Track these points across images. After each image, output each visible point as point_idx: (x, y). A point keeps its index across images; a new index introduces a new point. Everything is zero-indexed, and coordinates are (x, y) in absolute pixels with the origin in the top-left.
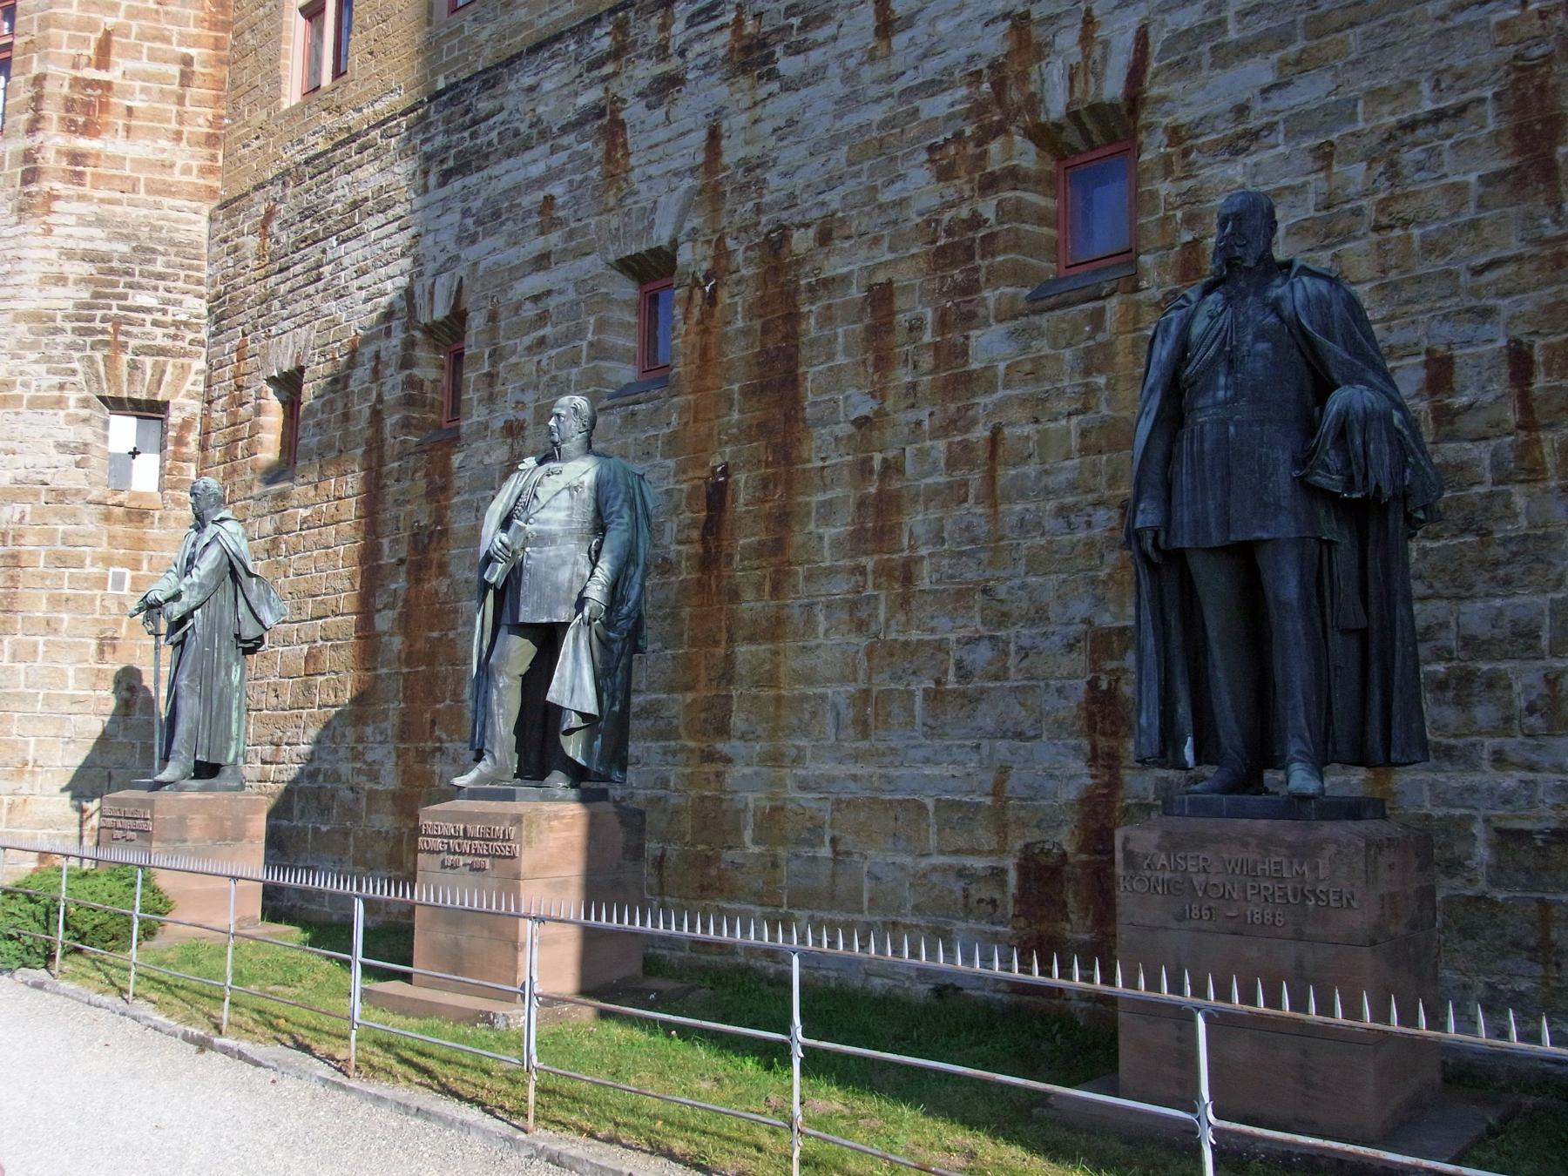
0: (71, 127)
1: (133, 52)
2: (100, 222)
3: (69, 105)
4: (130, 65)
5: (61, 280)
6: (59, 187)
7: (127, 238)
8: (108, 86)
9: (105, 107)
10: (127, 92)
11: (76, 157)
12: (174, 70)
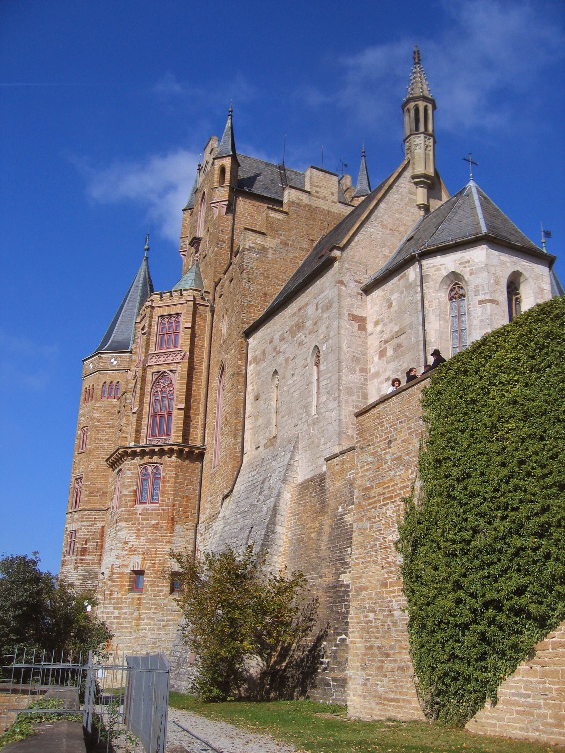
0: (82, 555)
1: (90, 542)
2: (84, 570)
3: (81, 551)
5: (79, 579)
8: (86, 548)
9: (86, 551)
10: (89, 548)
11: (82, 560)
12: (95, 544)
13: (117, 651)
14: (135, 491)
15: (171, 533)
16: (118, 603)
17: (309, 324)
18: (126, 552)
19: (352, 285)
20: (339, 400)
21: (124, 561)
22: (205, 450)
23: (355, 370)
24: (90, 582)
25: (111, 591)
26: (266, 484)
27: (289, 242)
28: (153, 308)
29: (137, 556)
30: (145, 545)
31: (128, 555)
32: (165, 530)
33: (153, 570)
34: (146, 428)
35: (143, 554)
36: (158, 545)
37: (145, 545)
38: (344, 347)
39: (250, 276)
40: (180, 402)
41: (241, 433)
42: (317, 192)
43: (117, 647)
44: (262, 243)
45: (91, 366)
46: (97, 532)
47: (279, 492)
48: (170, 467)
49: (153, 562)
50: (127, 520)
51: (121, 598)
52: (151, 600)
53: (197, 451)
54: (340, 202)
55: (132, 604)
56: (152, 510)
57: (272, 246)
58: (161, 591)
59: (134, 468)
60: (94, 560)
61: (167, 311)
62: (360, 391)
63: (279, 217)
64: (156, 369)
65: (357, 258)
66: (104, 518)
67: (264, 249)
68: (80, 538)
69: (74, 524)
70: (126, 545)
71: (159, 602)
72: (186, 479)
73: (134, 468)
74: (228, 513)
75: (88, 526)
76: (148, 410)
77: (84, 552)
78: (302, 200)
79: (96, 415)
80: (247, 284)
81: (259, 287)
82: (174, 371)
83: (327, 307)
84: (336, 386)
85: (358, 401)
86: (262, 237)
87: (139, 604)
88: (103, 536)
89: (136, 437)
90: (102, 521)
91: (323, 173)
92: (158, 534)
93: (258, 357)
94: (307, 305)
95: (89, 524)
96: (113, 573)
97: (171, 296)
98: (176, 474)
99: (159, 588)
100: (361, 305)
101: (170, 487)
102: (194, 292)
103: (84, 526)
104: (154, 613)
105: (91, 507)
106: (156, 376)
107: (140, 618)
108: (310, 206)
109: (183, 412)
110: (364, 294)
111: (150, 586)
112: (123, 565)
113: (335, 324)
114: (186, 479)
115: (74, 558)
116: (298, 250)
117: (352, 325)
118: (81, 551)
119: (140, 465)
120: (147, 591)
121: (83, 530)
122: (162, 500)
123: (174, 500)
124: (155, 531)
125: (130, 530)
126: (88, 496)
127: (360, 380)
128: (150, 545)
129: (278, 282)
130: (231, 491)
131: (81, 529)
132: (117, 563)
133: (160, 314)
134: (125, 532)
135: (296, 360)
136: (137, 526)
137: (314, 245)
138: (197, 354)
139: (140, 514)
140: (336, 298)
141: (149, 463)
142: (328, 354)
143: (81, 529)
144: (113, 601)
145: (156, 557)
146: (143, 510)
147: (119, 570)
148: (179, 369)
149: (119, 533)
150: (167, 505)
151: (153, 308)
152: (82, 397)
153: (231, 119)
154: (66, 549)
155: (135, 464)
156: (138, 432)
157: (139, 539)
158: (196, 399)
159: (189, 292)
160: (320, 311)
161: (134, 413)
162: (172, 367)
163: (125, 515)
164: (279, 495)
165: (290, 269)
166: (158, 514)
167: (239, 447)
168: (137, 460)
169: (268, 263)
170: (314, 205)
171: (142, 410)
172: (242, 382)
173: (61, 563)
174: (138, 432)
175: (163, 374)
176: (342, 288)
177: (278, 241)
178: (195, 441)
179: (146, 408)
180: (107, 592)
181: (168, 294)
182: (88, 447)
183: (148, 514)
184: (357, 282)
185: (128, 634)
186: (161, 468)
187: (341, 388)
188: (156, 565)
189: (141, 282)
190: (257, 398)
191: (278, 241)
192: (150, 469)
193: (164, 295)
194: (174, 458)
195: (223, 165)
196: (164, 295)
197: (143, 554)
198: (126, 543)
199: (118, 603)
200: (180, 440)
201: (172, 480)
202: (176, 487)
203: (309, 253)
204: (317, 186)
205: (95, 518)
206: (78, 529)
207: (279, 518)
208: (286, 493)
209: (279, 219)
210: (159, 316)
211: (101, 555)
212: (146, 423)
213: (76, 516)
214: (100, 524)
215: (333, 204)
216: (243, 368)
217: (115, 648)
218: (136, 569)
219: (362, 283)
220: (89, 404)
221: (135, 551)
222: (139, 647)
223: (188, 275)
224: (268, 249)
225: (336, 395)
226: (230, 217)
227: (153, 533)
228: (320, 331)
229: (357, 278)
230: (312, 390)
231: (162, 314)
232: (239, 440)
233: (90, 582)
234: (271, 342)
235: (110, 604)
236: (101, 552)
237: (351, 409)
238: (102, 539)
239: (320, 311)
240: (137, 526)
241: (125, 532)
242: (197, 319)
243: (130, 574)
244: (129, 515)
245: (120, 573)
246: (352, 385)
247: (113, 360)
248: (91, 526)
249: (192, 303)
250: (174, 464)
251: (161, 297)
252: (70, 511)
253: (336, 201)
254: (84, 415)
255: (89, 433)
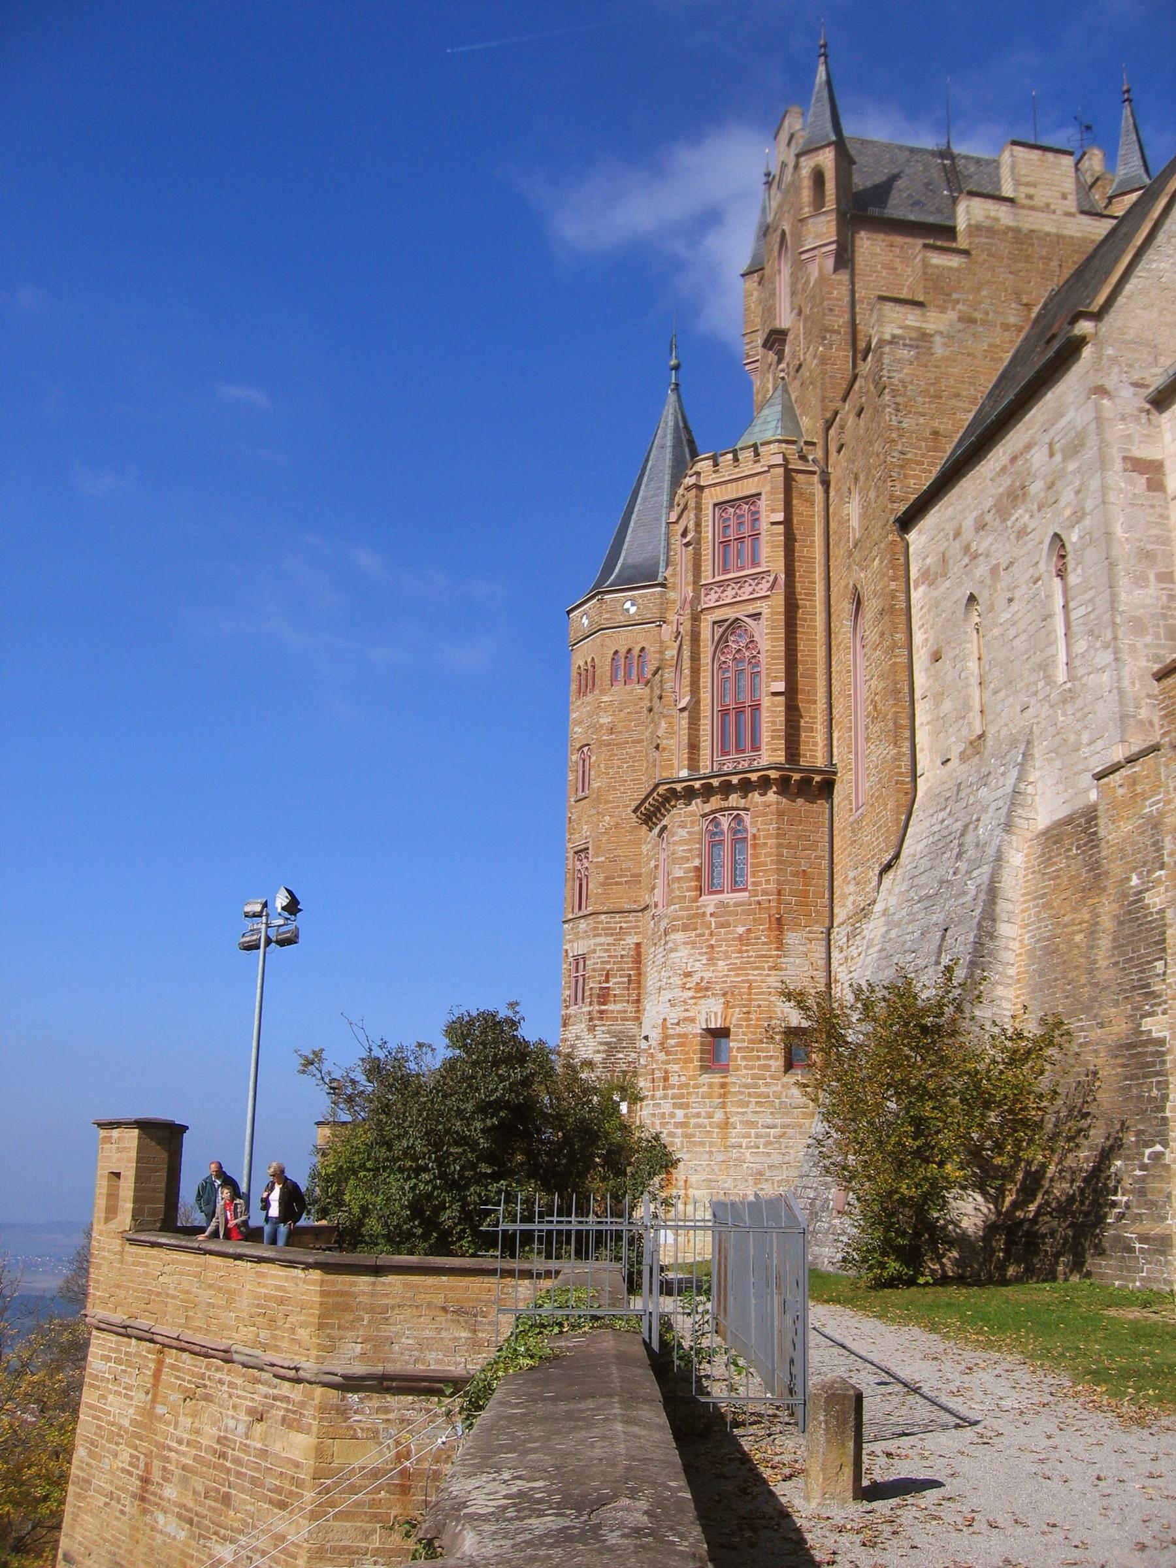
1: (615, 976)
2: (608, 1032)
3: (599, 996)
4: (615, 980)
5: (599, 1052)
6: (597, 1022)
7: (614, 1037)
8: (608, 988)
9: (608, 995)
10: (614, 989)
11: (601, 1012)
12: (626, 979)
13: (686, 1189)
14: (698, 869)
15: (778, 949)
16: (682, 1096)
17: (1036, 488)
18: (690, 994)
19: (1127, 392)
20: (1115, 648)
21: (687, 1010)
22: (835, 773)
23: (1148, 579)
24: (621, 1056)
25: (666, 1072)
26: (970, 838)
27: (978, 316)
28: (700, 488)
29: (712, 1000)
30: (727, 976)
31: (694, 998)
32: (764, 943)
33: (748, 1026)
34: (709, 738)
35: (724, 995)
36: (753, 975)
37: (727, 976)
38: (1119, 531)
39: (899, 399)
40: (775, 679)
41: (907, 734)
42: (1030, 197)
43: (686, 1181)
44: (917, 324)
45: (585, 621)
46: (628, 956)
47: (999, 851)
48: (764, 814)
49: (745, 1010)
50: (685, 928)
51: (687, 1085)
52: (747, 1086)
53: (818, 778)
54: (1083, 212)
55: (710, 1096)
56: (737, 905)
57: (942, 328)
58: (766, 1067)
59: (693, 822)
60: (626, 1011)
61: (731, 492)
62: (1161, 623)
63: (951, 264)
64: (718, 615)
65: (1132, 331)
66: (636, 927)
67: (924, 337)
68: (594, 970)
69: (581, 942)
70: (689, 979)
71: (763, 1089)
72: (799, 838)
73: (693, 822)
74: (893, 901)
75: (608, 944)
76: (709, 700)
77: (604, 996)
78: (997, 220)
79: (605, 720)
80: (894, 418)
81: (922, 420)
82: (756, 616)
83: (1074, 449)
84: (1107, 617)
85: (1159, 646)
86: (918, 311)
87: (724, 1095)
88: (639, 962)
89: (690, 759)
90: (636, 933)
91: (1039, 152)
92: (751, 953)
93: (932, 571)
94: (1028, 447)
95: (610, 940)
96: (666, 1037)
97: (736, 459)
98: (779, 828)
99: (763, 1062)
100: (1149, 436)
101: (769, 855)
102: (784, 445)
103: (600, 944)
104: (756, 1112)
105: (611, 907)
106: (721, 630)
107: (727, 1123)
108: (1017, 230)
109: (782, 699)
110: (1153, 411)
111: (744, 1058)
112: (685, 1019)
113: (1094, 484)
114: (799, 838)
115: (586, 1009)
116: (998, 329)
117: (1131, 482)
118: (599, 996)
119: (704, 816)
120: (738, 1069)
121: (598, 954)
122: (755, 884)
123: (779, 882)
124: (744, 948)
125: (693, 948)
126: (603, 884)
127: (1158, 598)
128: (737, 975)
129: (960, 404)
130: (897, 856)
131: (594, 951)
132: (674, 1015)
133: (716, 501)
134: (684, 952)
135: (1014, 568)
136: (708, 940)
137: (1033, 315)
138: (801, 576)
139: (711, 915)
140: (1093, 426)
141: (722, 810)
142: (1083, 549)
143: (594, 951)
144: (670, 1092)
145: (750, 1000)
146: (717, 906)
147: (679, 1030)
148: (766, 611)
149: (673, 955)
150: (765, 893)
151: (700, 488)
152: (574, 687)
153: (826, 63)
154: (568, 993)
155: (692, 814)
156: (694, 747)
157: (715, 965)
158: (808, 669)
159: (774, 447)
160: (1058, 457)
161: (682, 710)
162: (751, 609)
163: (682, 918)
164: (999, 858)
165: (985, 374)
166: (749, 913)
167: (906, 761)
168: (697, 806)
169: (936, 367)
170: (1026, 226)
171: (698, 702)
172: (902, 627)
173: (561, 1022)
174: (694, 747)
175: (734, 625)
176: (1105, 401)
177: (952, 315)
178: (812, 756)
179: (705, 697)
180: (658, 1074)
181: (730, 456)
182: (595, 785)
183: (730, 913)
184: (1135, 385)
185: (706, 1157)
186: (747, 819)
187: (1118, 620)
188: (752, 1016)
189: (669, 437)
190: (936, 658)
191: (952, 315)
192: (725, 822)
193: (721, 459)
194: (771, 796)
195: (817, 166)
196: (721, 459)
197: (724, 995)
198: (688, 975)
199: (682, 1096)
200: (780, 758)
201: (772, 842)
202: (780, 855)
203: (1022, 335)
204: (1028, 184)
205: (621, 928)
206: (589, 952)
207: (1002, 906)
208: (1013, 852)
209: (951, 269)
210: (715, 505)
211: (638, 1001)
212: (709, 728)
213: (581, 926)
214: (631, 940)
215: (1068, 219)
216: (902, 597)
217: (681, 1183)
218: (713, 1026)
219: (1147, 386)
220: (589, 698)
221: (707, 989)
222: (730, 1180)
223: (766, 412)
224: (932, 336)
225: (1109, 636)
226: (844, 276)
227: (741, 952)
228: (1062, 503)
229: (1136, 376)
230: (1055, 631)
231: (721, 499)
232: (906, 747)
233: (621, 1056)
234: (957, 535)
235: (665, 1097)
236: (639, 995)
237: (1144, 664)
238: (638, 969)
239: (1058, 457)
240: (708, 940)
241: (684, 952)
242: (795, 502)
243: (702, 1036)
244: (690, 917)
245: (680, 1036)
246: (1141, 611)
247: (628, 605)
248: (614, 945)
249: (781, 470)
250: (774, 807)
251: (716, 464)
252: (570, 916)
253: (1073, 210)
254: (579, 722)
255: (593, 758)
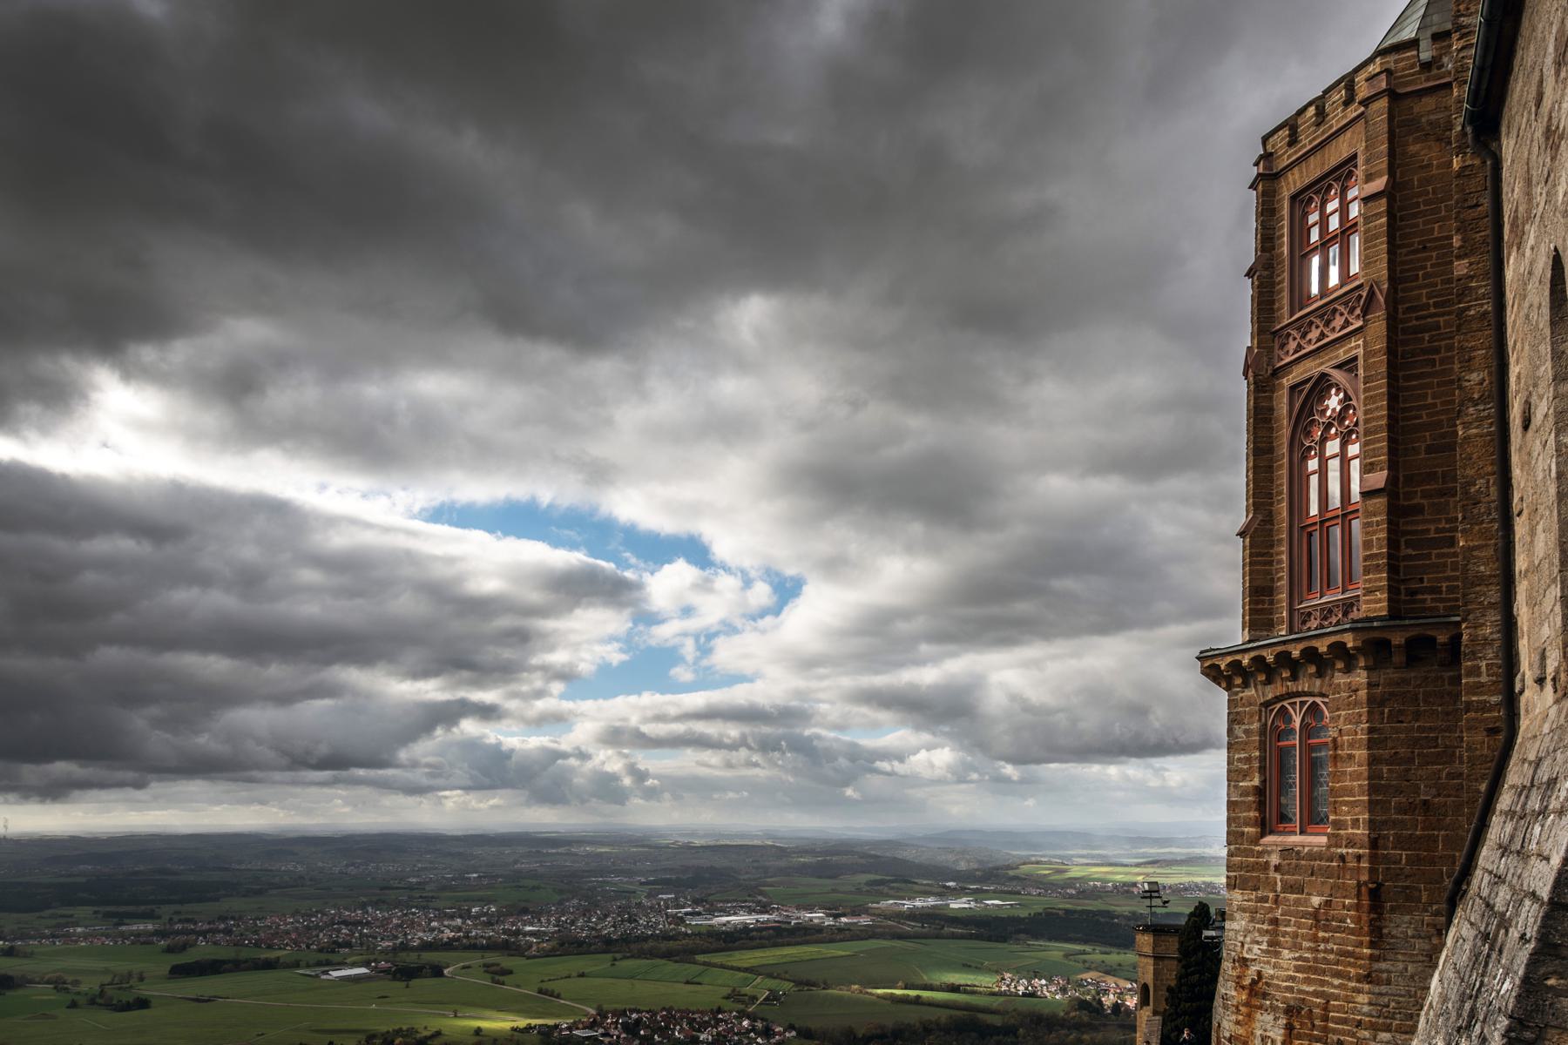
30: (1293, 979)
32: (1352, 932)
56: (1312, 856)
92: (1330, 946)
101: (1356, 776)
123: (1372, 824)
124: (1321, 934)
128: (1308, 981)
150: (1351, 843)
157: (1277, 954)
166: (1327, 872)
201: (1361, 754)
